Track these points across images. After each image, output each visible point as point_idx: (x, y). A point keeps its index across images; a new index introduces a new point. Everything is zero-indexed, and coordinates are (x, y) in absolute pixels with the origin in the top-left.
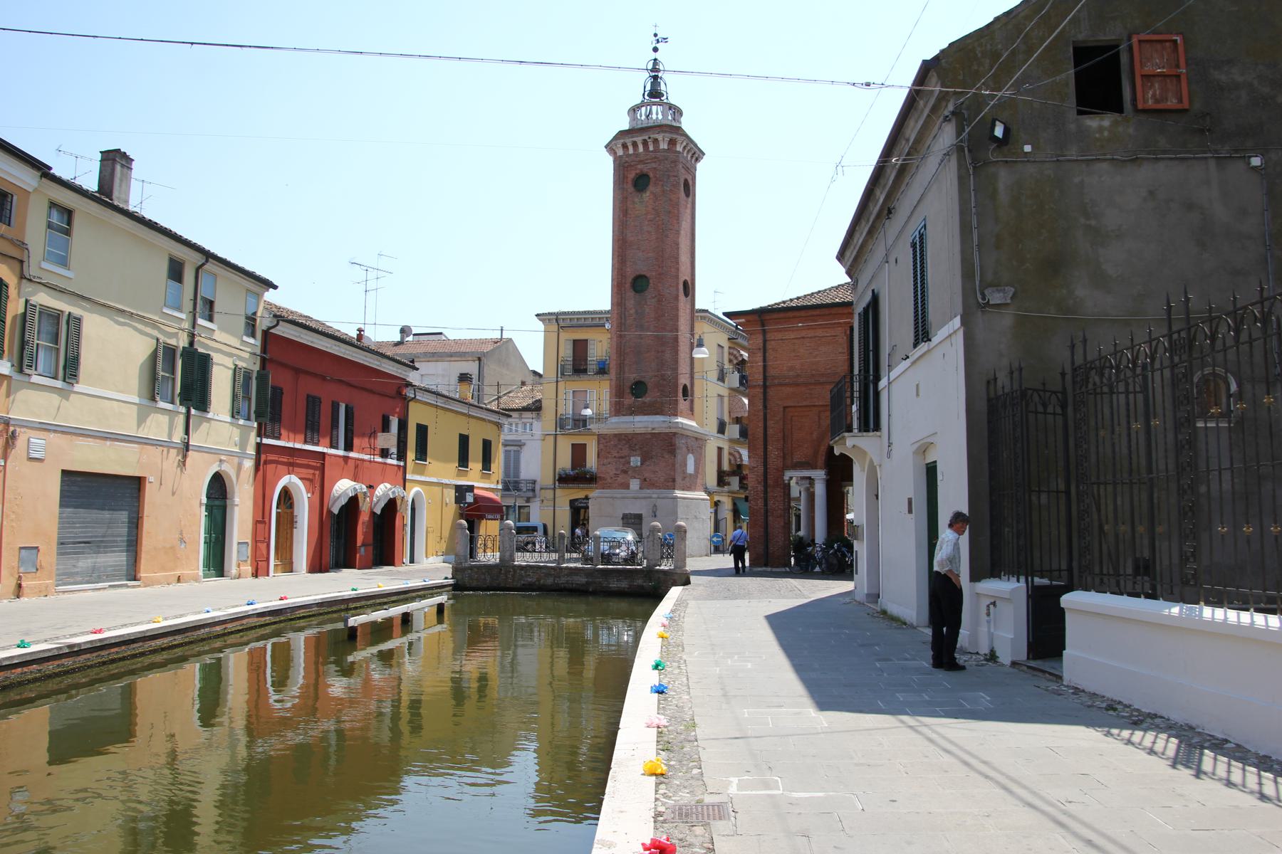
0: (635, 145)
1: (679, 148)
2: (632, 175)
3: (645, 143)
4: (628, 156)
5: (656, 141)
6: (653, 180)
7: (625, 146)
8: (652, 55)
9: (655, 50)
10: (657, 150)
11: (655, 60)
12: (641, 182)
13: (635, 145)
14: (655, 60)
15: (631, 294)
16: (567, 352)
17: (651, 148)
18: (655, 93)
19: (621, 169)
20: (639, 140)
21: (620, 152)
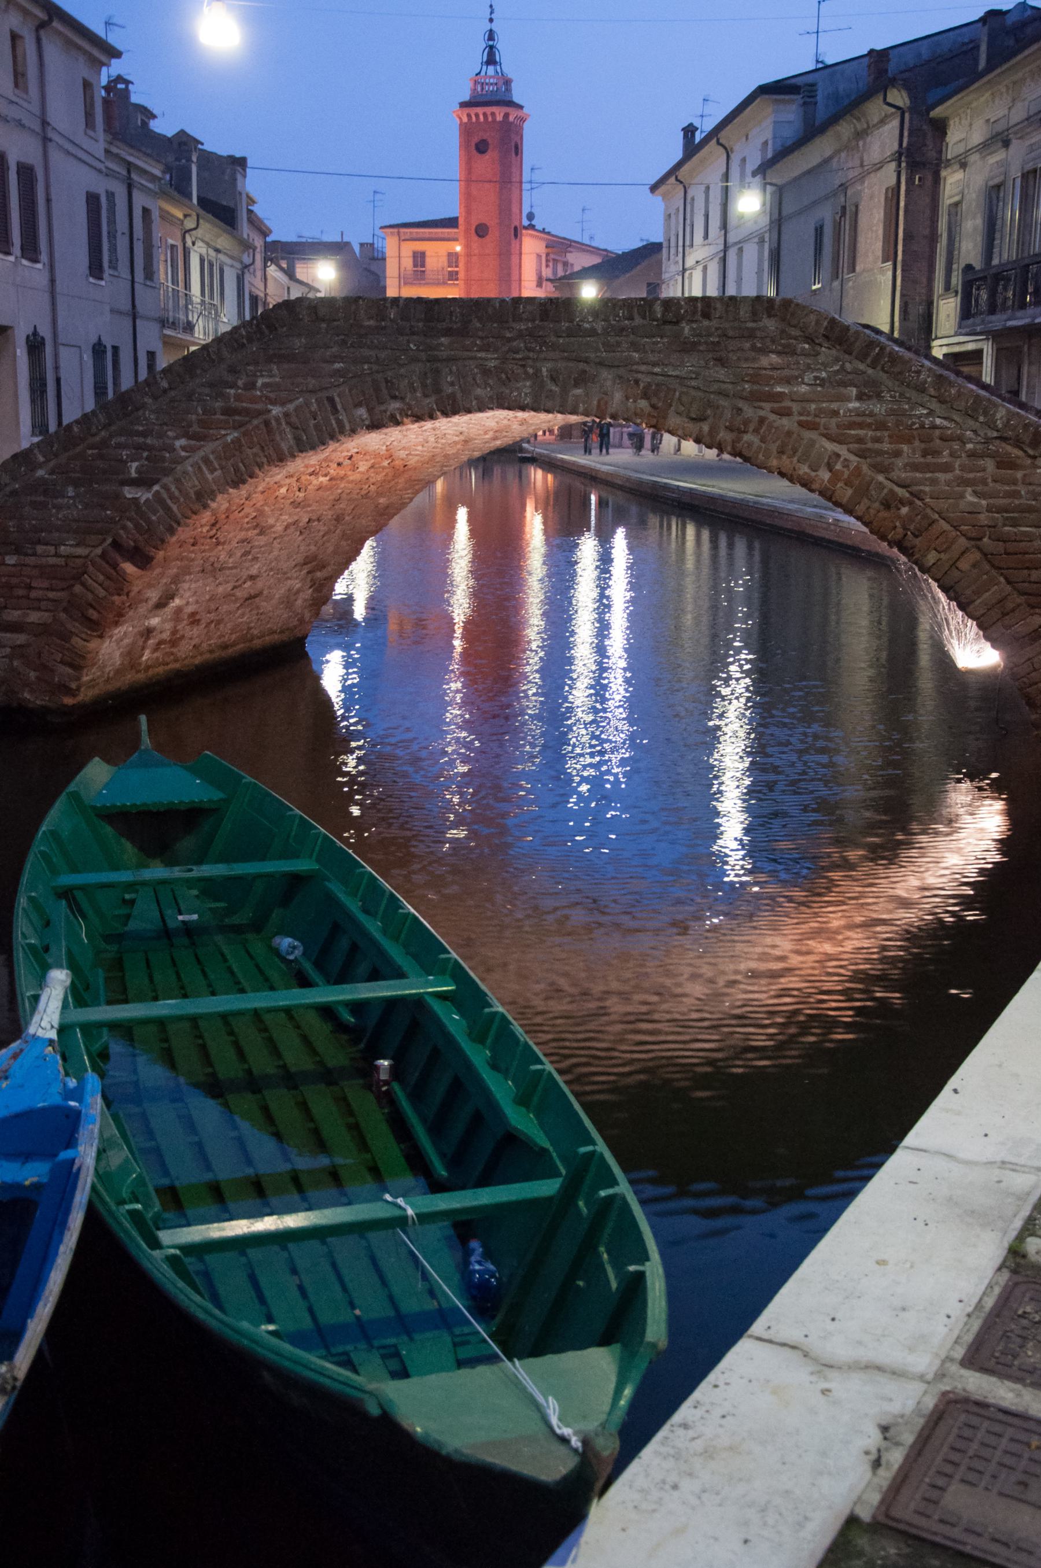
0: (477, 115)
1: (511, 119)
2: (475, 140)
3: (485, 115)
4: (472, 123)
5: (493, 114)
6: (491, 147)
7: (469, 116)
8: (488, 26)
9: (491, 20)
10: (494, 120)
11: (491, 30)
12: (482, 147)
13: (477, 115)
14: (491, 30)
15: (475, 238)
16: (408, 263)
17: (490, 119)
18: (491, 60)
19: (467, 131)
20: (480, 110)
21: (465, 119)
